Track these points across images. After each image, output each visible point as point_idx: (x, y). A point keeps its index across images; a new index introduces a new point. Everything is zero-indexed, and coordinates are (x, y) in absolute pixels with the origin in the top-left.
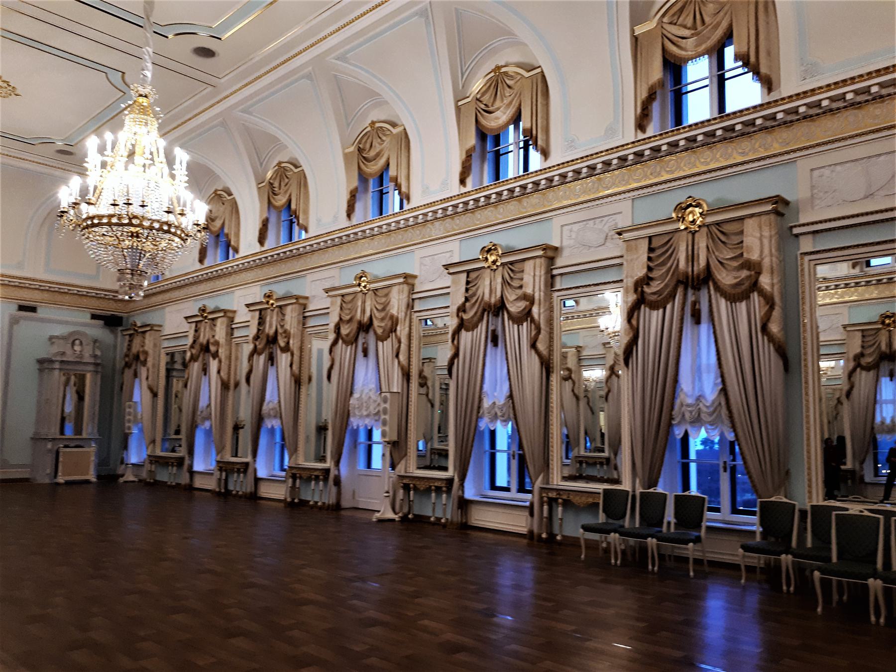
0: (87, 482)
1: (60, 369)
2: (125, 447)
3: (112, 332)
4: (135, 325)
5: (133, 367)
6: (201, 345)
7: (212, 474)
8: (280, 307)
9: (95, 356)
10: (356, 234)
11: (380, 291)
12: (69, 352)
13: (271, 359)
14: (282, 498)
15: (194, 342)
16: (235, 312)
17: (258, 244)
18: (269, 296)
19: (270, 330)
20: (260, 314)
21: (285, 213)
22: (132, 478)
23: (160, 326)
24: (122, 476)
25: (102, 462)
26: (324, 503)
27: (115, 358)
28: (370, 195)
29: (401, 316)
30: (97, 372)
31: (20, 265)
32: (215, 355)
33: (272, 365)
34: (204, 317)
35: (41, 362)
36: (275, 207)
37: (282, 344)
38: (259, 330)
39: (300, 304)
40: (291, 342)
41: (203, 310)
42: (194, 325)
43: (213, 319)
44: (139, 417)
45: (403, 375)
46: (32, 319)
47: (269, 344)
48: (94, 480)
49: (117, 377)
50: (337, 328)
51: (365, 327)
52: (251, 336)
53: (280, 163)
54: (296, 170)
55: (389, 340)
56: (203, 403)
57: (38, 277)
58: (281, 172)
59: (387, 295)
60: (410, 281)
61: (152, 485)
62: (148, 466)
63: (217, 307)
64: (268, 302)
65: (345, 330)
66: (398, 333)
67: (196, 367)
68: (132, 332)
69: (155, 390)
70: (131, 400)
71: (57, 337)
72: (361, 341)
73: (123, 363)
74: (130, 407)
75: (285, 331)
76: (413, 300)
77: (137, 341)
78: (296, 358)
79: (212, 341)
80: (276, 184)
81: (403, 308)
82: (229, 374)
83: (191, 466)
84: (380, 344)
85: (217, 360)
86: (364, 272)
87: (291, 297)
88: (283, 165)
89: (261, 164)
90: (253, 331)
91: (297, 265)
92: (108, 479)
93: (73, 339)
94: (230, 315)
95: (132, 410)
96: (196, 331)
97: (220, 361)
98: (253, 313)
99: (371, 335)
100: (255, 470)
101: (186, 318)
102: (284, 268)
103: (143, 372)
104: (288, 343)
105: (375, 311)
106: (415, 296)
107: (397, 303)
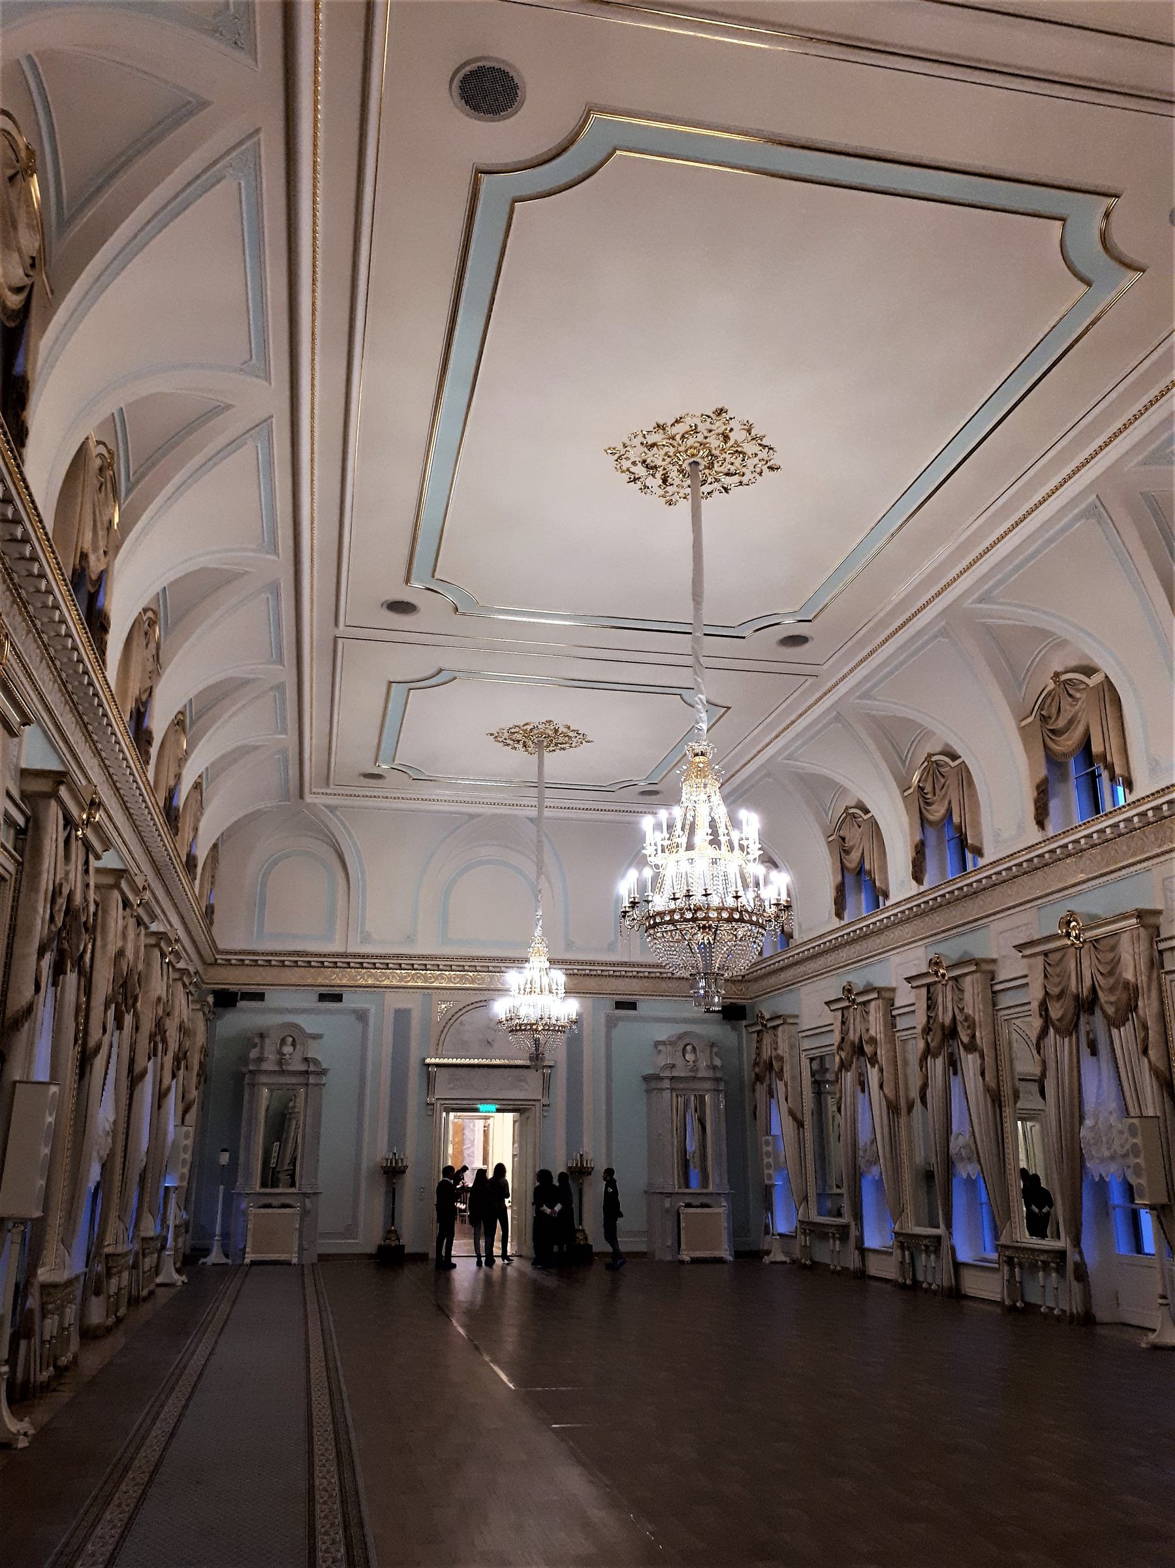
0: (720, 1261)
1: (672, 1089)
2: (769, 1208)
3: (734, 1028)
4: (763, 1018)
7: (891, 1254)
8: (956, 979)
9: (714, 1068)
10: (1053, 851)
11: (1103, 942)
12: (679, 1062)
13: (953, 1064)
14: (998, 1298)
15: (843, 1039)
17: (914, 883)
18: (936, 964)
21: (947, 833)
22: (781, 1257)
23: (797, 1016)
24: (768, 1253)
25: (739, 1229)
26: (1064, 1311)
28: (1072, 782)
29: (1143, 980)
30: (718, 1091)
31: (611, 947)
32: (873, 1060)
33: (955, 1073)
34: (851, 1000)
35: (647, 1079)
36: (931, 823)
37: (965, 1039)
38: (929, 1017)
40: (978, 1034)
41: (848, 990)
42: (839, 1013)
43: (865, 1003)
44: (782, 1159)
45: (1161, 1086)
46: (635, 1019)
47: (946, 1038)
48: (730, 1258)
49: (747, 1094)
50: (1044, 1007)
51: (1088, 1004)
52: (919, 1030)
53: (930, 755)
54: (953, 764)
55: (1129, 1024)
56: (864, 1138)
57: (634, 959)
58: (933, 769)
59: (1113, 948)
60: (1151, 920)
61: (808, 1269)
62: (801, 1238)
63: (869, 984)
64: (936, 973)
65: (1055, 1012)
66: (1141, 1012)
67: (849, 1077)
68: (759, 1028)
69: (799, 1116)
70: (768, 1133)
71: (663, 1043)
72: (1083, 1028)
74: (767, 1143)
75: (967, 1018)
76: (1161, 952)
77: (767, 1039)
79: (865, 1037)
80: (928, 789)
81: (1143, 967)
82: (897, 1089)
83: (860, 1239)
84: (1115, 1032)
86: (1072, 913)
88: (934, 758)
89: (904, 762)
90: (920, 1020)
91: (973, 909)
92: (749, 1257)
93: (683, 1043)
94: (887, 995)
95: (770, 1149)
96: (843, 1023)
99: (1098, 1019)
100: (953, 1249)
101: (828, 1003)
102: (955, 915)
104: (973, 1036)
105: (1099, 977)
106: (1162, 946)
107: (1131, 962)
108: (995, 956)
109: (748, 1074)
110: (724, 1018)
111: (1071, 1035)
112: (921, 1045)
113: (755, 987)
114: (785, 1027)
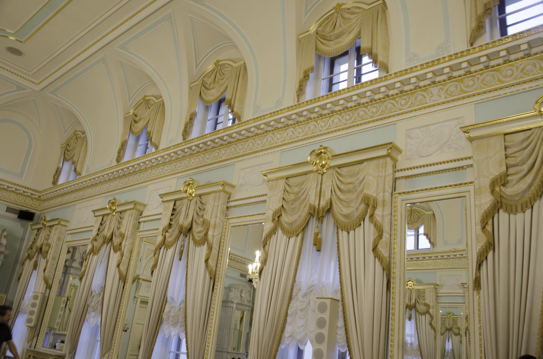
4: (45, 220)
5: (35, 259)
6: (105, 238)
16: (145, 206)
19: (183, 221)
20: (175, 205)
23: (67, 221)
27: (19, 251)
32: (118, 248)
43: (121, 212)
73: (26, 255)
77: (43, 234)
79: (117, 233)
85: (119, 253)
87: (216, 184)
90: (165, 222)
97: (122, 255)
98: (167, 204)
101: (94, 211)
103: (42, 263)
108: (234, 183)
109: (23, 254)
110: (19, 217)
112: (160, 239)
113: (46, 204)
114: (59, 226)
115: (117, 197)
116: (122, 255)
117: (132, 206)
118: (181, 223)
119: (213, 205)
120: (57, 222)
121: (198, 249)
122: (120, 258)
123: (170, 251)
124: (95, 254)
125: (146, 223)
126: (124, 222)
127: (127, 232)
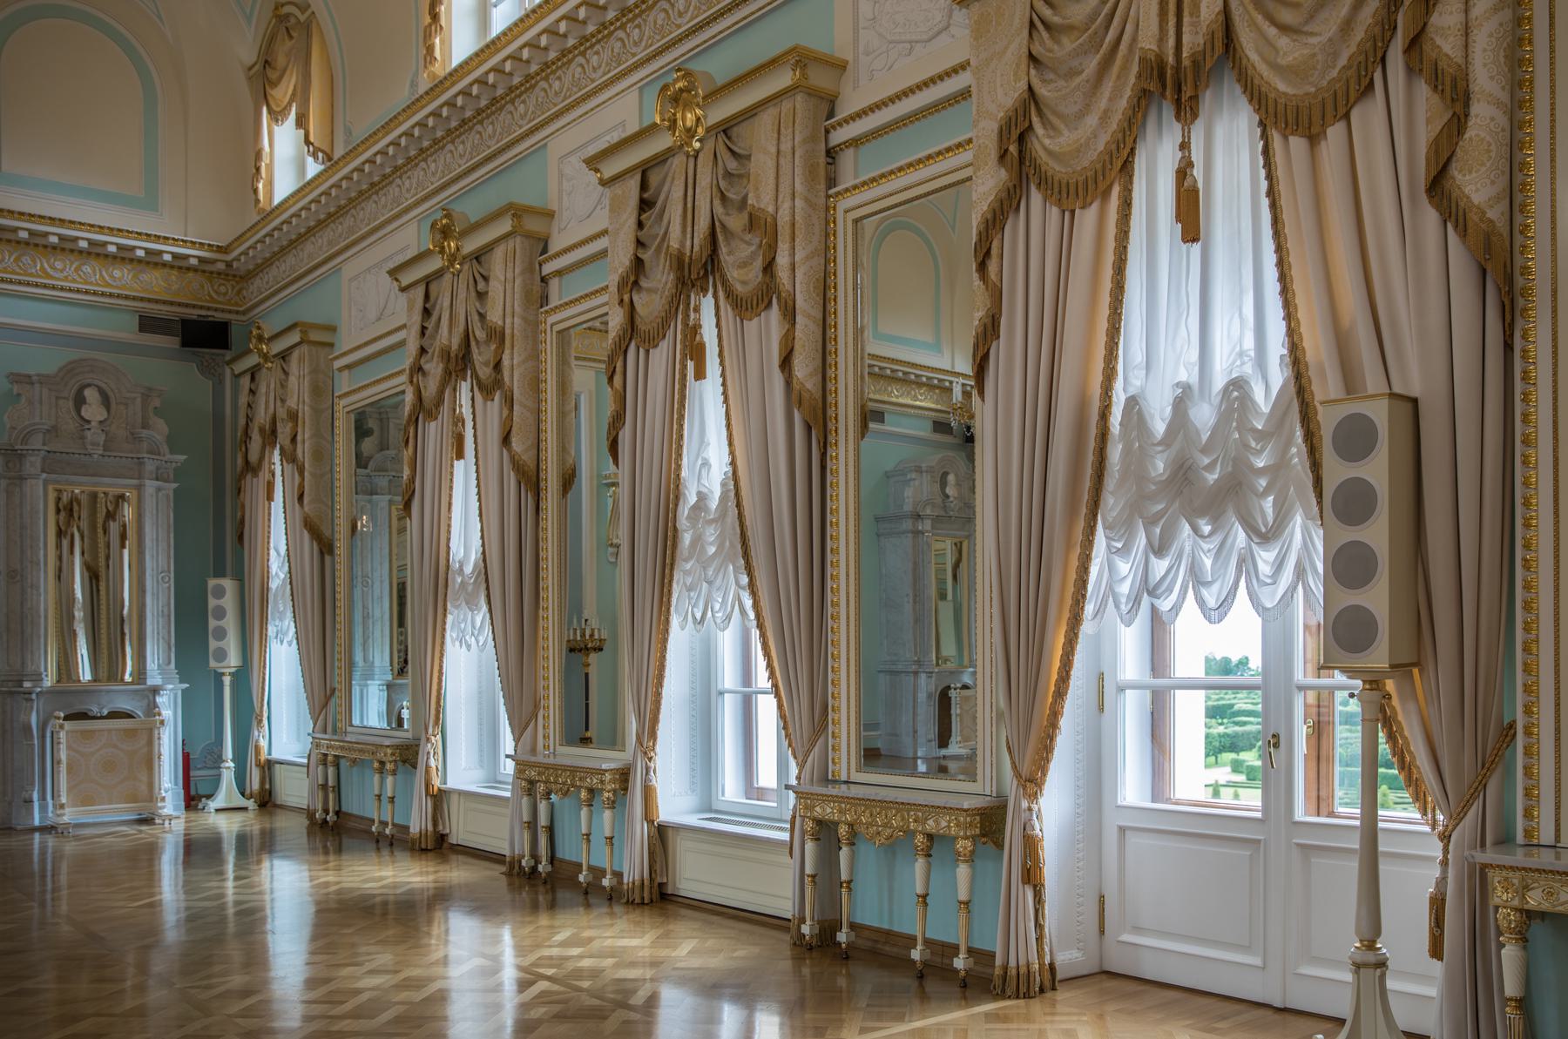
3: (206, 370)
4: (260, 339)
8: (725, 129)
20: (644, 186)
39: (813, 93)
69: (327, 533)
78: (805, 328)
90: (621, 258)
97: (509, 401)
98: (618, 189)
108: (842, 51)
111: (1106, 194)
112: (616, 319)
114: (305, 348)
115: (457, 208)
116: (509, 401)
117: (505, 226)
118: (675, 244)
119: (773, 150)
120: (295, 337)
121: (752, 326)
122: (506, 412)
123: (660, 356)
124: (432, 415)
125: (566, 278)
126: (495, 288)
127: (508, 321)
